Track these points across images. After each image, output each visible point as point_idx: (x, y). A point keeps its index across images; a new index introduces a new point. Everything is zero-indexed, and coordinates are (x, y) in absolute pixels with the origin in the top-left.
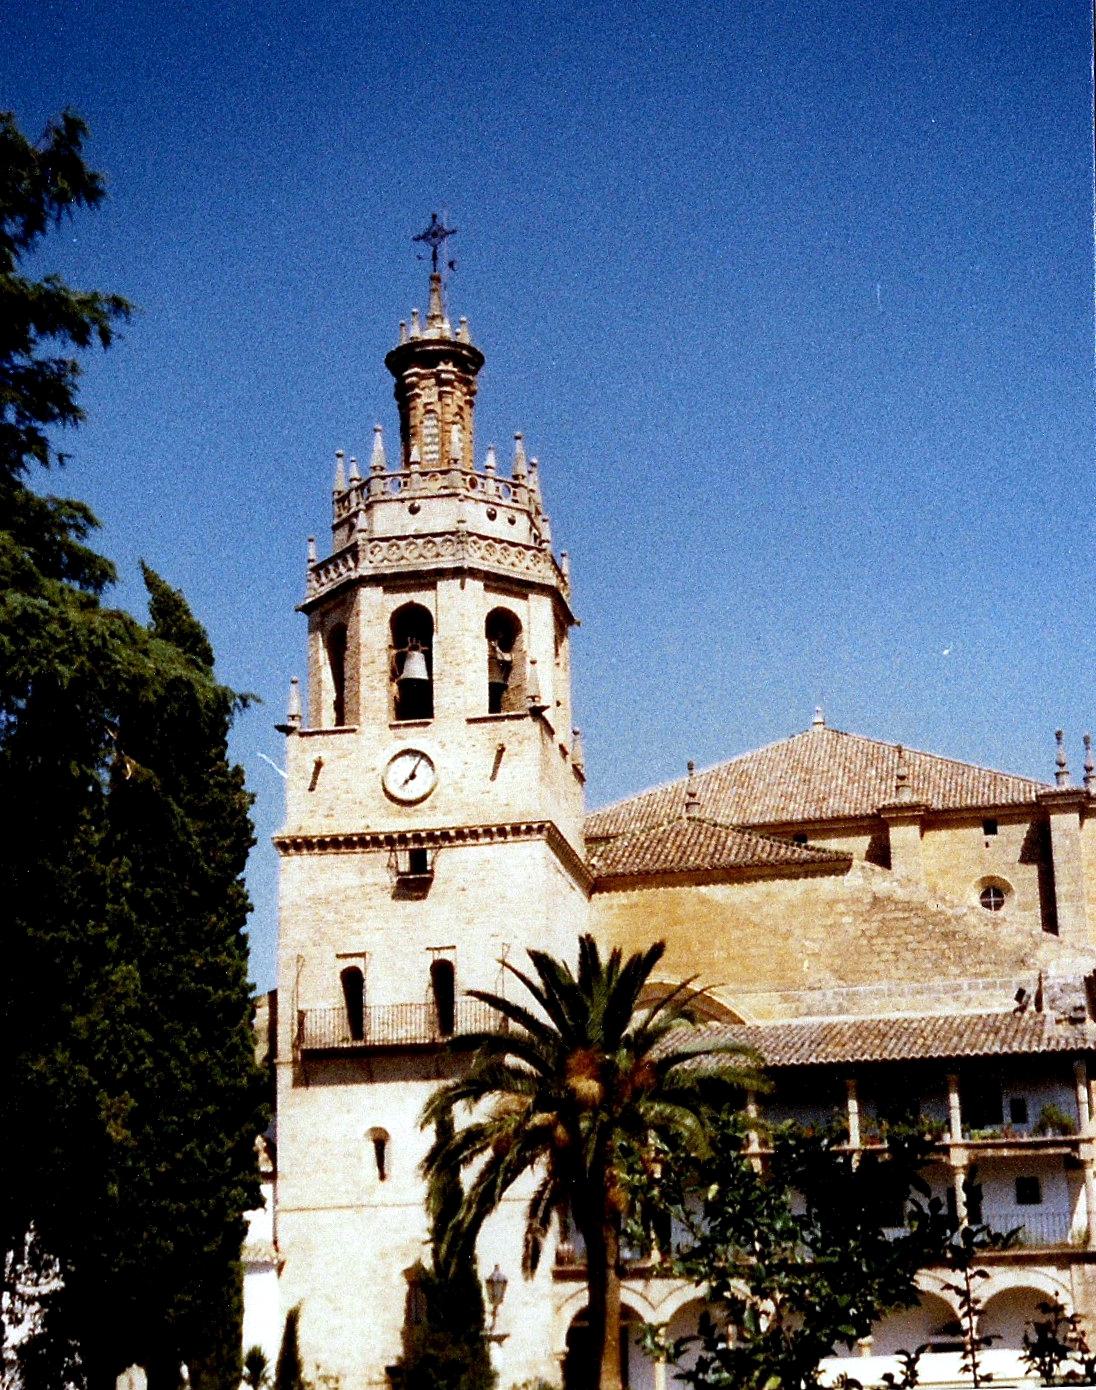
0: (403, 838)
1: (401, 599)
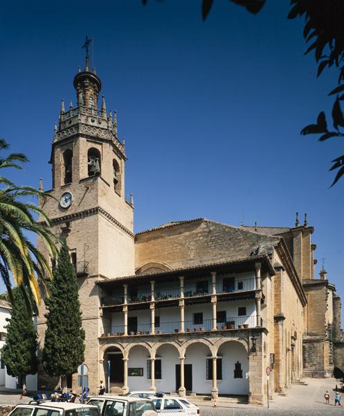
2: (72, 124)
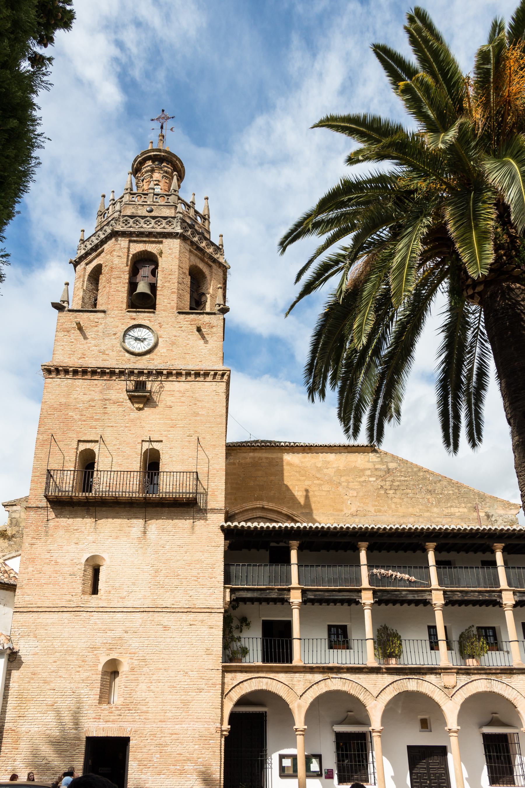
0: (132, 373)
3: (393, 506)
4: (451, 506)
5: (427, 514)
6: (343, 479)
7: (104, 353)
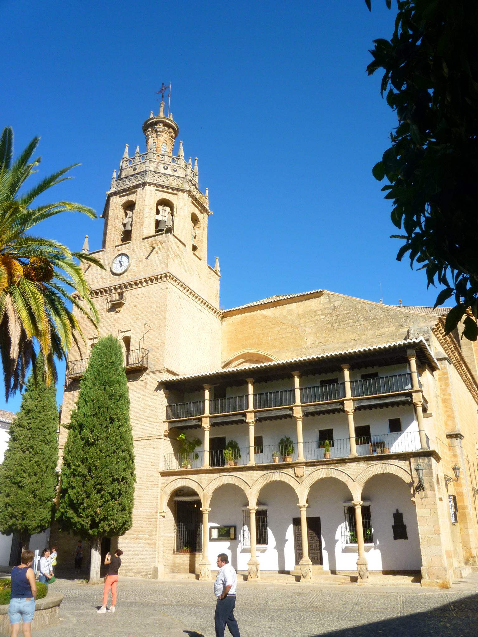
1: (126, 199)
2: (137, 171)
3: (338, 335)
4: (382, 328)
5: (363, 337)
6: (302, 321)
7: (103, 278)
